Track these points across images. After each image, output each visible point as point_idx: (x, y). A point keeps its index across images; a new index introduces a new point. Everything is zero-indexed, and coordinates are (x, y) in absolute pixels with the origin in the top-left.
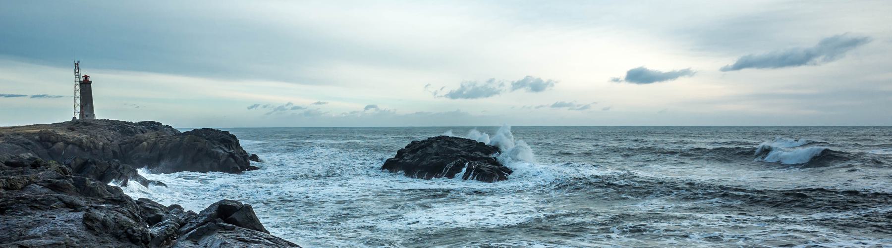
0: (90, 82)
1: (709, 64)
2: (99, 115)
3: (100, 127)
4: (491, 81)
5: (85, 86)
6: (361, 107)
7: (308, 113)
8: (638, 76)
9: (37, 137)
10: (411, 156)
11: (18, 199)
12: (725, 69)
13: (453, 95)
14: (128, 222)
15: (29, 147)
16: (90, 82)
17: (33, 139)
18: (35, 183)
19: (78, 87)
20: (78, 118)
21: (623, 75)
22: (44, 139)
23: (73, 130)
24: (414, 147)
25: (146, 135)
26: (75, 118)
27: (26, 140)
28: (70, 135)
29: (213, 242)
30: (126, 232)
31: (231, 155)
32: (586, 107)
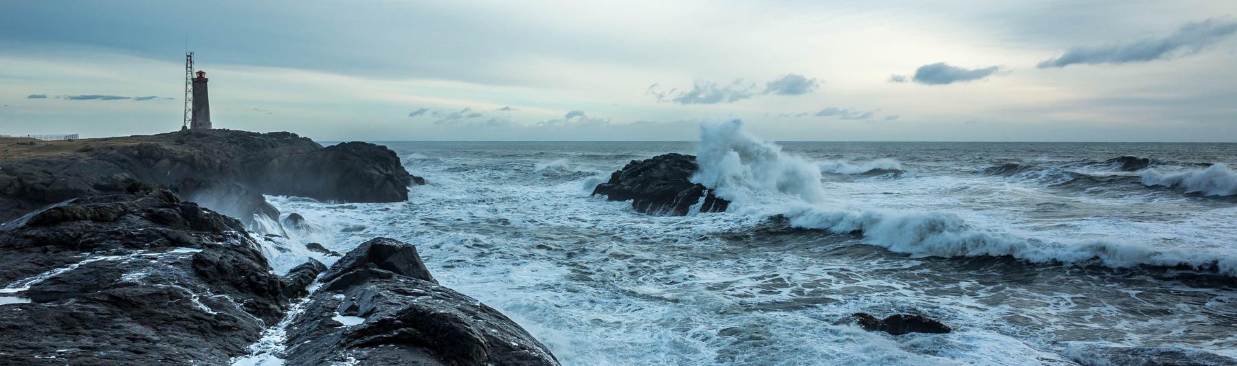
0: (206, 80)
1: (1026, 58)
2: (218, 121)
3: (216, 139)
4: (737, 82)
5: (200, 84)
6: (561, 114)
7: (492, 122)
8: (932, 75)
9: (136, 152)
10: (630, 180)
11: (110, 233)
12: (1043, 66)
13: (688, 99)
14: (251, 267)
15: (125, 165)
16: (206, 80)
17: (130, 155)
18: (133, 213)
19: (190, 87)
20: (189, 127)
21: (911, 72)
22: (142, 153)
23: (182, 143)
24: (635, 169)
25: (277, 150)
26: (184, 127)
27: (122, 156)
28: (178, 149)
29: (362, 295)
30: (248, 279)
31: (389, 178)
32: (865, 116)
